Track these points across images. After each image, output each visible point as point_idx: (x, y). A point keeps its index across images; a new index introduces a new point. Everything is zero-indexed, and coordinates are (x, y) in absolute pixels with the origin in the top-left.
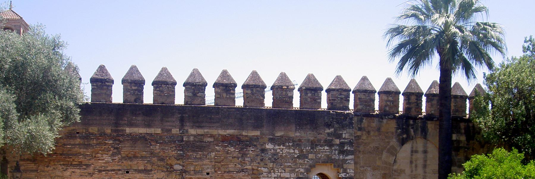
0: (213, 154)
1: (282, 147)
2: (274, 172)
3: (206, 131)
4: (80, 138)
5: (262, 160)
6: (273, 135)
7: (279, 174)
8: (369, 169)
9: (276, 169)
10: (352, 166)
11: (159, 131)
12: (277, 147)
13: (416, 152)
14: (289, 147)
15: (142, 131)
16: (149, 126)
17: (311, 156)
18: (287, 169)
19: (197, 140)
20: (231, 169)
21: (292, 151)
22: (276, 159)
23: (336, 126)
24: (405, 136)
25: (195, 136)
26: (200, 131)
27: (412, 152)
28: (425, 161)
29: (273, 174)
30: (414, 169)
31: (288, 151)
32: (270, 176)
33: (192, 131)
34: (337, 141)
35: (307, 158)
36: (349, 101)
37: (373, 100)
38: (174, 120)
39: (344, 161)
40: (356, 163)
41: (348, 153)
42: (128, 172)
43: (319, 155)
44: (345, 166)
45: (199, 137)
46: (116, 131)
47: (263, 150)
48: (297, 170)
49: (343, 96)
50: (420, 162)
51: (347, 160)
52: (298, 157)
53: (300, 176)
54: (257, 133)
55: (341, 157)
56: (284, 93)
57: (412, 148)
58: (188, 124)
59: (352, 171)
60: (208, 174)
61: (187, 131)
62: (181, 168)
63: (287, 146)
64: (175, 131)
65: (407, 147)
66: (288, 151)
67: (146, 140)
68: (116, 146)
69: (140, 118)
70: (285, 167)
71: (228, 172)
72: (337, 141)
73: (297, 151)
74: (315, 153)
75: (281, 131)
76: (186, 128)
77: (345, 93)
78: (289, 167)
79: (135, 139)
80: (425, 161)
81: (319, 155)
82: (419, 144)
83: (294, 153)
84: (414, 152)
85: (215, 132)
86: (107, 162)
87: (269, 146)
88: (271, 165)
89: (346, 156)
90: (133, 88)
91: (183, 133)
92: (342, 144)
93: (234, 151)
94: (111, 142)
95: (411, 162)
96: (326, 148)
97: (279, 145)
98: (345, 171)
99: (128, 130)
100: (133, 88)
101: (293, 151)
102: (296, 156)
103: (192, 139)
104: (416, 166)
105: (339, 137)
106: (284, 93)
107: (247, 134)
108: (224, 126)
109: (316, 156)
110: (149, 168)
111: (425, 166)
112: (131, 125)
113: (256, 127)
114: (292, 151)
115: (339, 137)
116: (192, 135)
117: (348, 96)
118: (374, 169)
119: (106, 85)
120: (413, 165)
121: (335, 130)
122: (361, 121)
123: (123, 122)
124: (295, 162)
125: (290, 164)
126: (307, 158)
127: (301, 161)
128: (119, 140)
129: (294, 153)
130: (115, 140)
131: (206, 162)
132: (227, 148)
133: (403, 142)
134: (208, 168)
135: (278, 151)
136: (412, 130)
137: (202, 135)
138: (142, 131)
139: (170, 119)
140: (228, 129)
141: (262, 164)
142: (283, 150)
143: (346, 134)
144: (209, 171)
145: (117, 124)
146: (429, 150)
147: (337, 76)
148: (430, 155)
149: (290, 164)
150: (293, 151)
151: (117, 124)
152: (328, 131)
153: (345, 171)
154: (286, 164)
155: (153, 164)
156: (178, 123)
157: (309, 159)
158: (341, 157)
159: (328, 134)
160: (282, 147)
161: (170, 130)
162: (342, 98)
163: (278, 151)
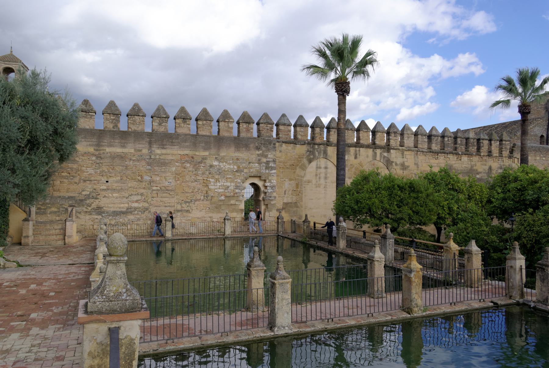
0: (174, 169)
1: (224, 164)
5: (210, 173)
6: (219, 155)
7: (222, 183)
8: (287, 180)
9: (220, 180)
10: (275, 178)
11: (132, 151)
12: (221, 164)
13: (320, 168)
14: (230, 164)
16: (123, 147)
17: (245, 171)
18: (229, 180)
22: (221, 172)
23: (264, 149)
24: (312, 157)
25: (160, 155)
26: (164, 151)
27: (317, 168)
28: (326, 174)
30: (318, 180)
31: (229, 166)
33: (158, 151)
34: (264, 160)
35: (243, 171)
36: (272, 131)
37: (290, 131)
38: (144, 142)
39: (269, 174)
40: (277, 176)
41: (272, 168)
43: (252, 170)
44: (270, 178)
47: (211, 166)
48: (236, 180)
49: (268, 128)
50: (323, 175)
51: (271, 173)
52: (236, 171)
54: (207, 153)
55: (267, 171)
57: (317, 165)
58: (155, 146)
59: (274, 181)
61: (154, 151)
62: (150, 178)
64: (145, 151)
65: (314, 164)
66: (229, 166)
71: (185, 182)
72: (264, 160)
73: (236, 167)
76: (153, 149)
77: (270, 126)
78: (230, 178)
79: (114, 157)
80: (326, 174)
81: (252, 170)
82: (322, 162)
84: (318, 167)
85: (175, 152)
86: (91, 174)
87: (216, 163)
88: (217, 177)
89: (271, 170)
90: (112, 117)
91: (151, 152)
92: (268, 163)
95: (316, 175)
96: (257, 165)
97: (222, 163)
98: (270, 181)
99: (108, 150)
100: (112, 117)
103: (158, 157)
104: (320, 178)
105: (266, 156)
111: (326, 178)
112: (110, 146)
113: (205, 149)
114: (232, 167)
115: (266, 156)
117: (272, 128)
118: (291, 180)
119: (89, 115)
120: (318, 177)
121: (263, 152)
122: (281, 146)
123: (104, 144)
126: (243, 171)
131: (169, 174)
132: (185, 164)
133: (310, 161)
135: (222, 166)
136: (317, 153)
139: (141, 142)
141: (210, 176)
142: (225, 166)
143: (271, 156)
146: (329, 167)
147: (264, 114)
148: (329, 170)
151: (98, 145)
152: (258, 152)
153: (270, 181)
156: (147, 145)
158: (267, 171)
159: (258, 155)
160: (224, 164)
161: (140, 151)
162: (268, 129)
163: (222, 166)
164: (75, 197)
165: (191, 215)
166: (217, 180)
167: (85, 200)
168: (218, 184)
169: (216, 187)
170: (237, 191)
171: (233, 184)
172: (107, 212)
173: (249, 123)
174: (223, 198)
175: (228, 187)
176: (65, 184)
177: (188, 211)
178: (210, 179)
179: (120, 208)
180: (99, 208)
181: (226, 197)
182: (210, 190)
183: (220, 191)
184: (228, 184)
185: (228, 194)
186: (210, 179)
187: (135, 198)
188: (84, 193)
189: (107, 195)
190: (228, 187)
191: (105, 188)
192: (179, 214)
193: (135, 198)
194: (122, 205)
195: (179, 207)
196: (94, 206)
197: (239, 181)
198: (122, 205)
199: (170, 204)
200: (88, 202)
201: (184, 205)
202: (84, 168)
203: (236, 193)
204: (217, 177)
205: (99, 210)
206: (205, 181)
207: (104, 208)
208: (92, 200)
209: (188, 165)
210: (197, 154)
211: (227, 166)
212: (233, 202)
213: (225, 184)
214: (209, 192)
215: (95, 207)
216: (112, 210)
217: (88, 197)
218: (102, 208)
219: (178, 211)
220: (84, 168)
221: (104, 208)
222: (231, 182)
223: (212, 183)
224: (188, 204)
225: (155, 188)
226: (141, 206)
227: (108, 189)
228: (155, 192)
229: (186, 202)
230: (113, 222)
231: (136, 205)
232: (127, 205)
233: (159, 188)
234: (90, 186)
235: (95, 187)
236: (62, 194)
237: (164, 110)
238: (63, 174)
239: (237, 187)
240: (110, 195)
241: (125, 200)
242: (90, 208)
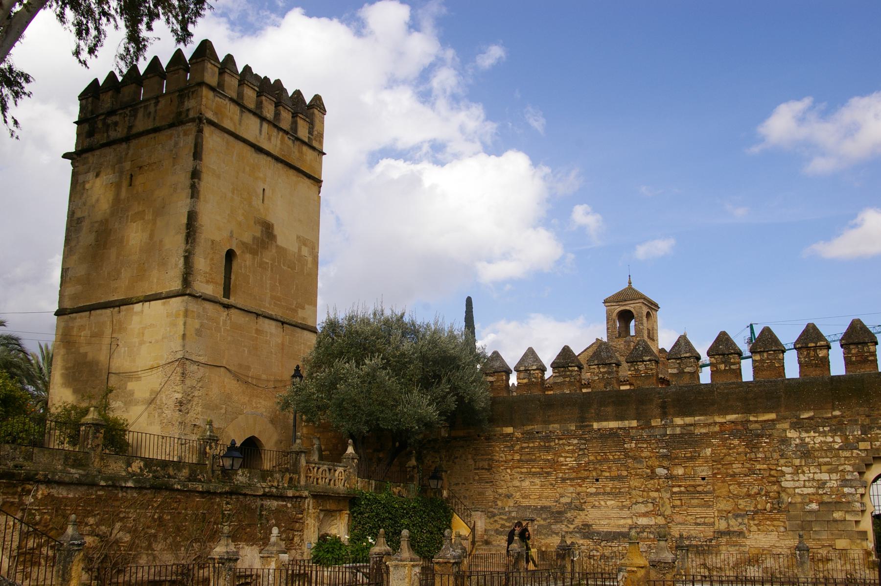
0: (708, 451)
1: (812, 434)
2: (803, 473)
3: (697, 418)
4: (540, 438)
7: (811, 475)
9: (805, 469)
12: (804, 435)
14: (824, 434)
15: (613, 424)
16: (622, 418)
17: (862, 445)
18: (824, 468)
19: (685, 432)
20: (737, 471)
21: (830, 439)
22: (806, 453)
26: (688, 420)
29: (801, 475)
31: (823, 439)
32: (796, 478)
33: (678, 421)
42: (597, 480)
45: (689, 428)
46: (581, 427)
48: (841, 468)
53: (847, 477)
56: (812, 353)
60: (703, 479)
63: (820, 432)
66: (823, 439)
67: (618, 436)
68: (582, 447)
69: (609, 409)
70: (819, 465)
73: (838, 439)
74: (871, 440)
75: (810, 409)
78: (825, 464)
83: (834, 442)
87: (791, 434)
88: (797, 462)
93: (739, 445)
94: (576, 441)
97: (807, 432)
99: (596, 426)
101: (831, 440)
102: (837, 447)
103: (678, 431)
106: (812, 353)
107: (755, 419)
108: (724, 412)
109: (871, 445)
110: (625, 473)
112: (599, 419)
114: (830, 439)
116: (678, 426)
119: (569, 371)
124: (838, 456)
125: (828, 459)
127: (847, 454)
128: (585, 439)
129: (834, 442)
130: (581, 439)
134: (703, 471)
135: (807, 440)
137: (691, 425)
138: (613, 424)
140: (728, 414)
141: (782, 461)
142: (814, 439)
144: (704, 474)
145: (582, 419)
149: (828, 459)
150: (831, 440)
151: (582, 419)
154: (821, 460)
155: (627, 468)
157: (861, 450)
160: (812, 434)
163: (807, 440)
164: (550, 507)
165: (748, 543)
166: (797, 470)
167: (565, 512)
168: (802, 477)
169: (797, 484)
170: (846, 490)
171: (834, 476)
172: (599, 533)
173: (865, 343)
174: (814, 506)
175: (825, 483)
176: (537, 487)
177: (740, 534)
178: (784, 468)
179: (619, 526)
180: (587, 525)
181: (821, 503)
182: (784, 489)
183: (806, 491)
184: (825, 477)
185: (826, 499)
186: (784, 468)
187: (642, 509)
188: (563, 500)
189: (597, 504)
190: (825, 483)
191: (593, 490)
192: (723, 540)
193: (642, 509)
194: (622, 522)
195: (722, 525)
196: (578, 522)
197: (849, 468)
198: (622, 522)
199: (707, 520)
200: (569, 515)
201: (732, 522)
202: (562, 459)
203: (844, 495)
204: (797, 462)
205: (586, 531)
206: (773, 472)
207: (594, 527)
208: (575, 513)
209: (736, 442)
210: (752, 418)
211: (819, 439)
212: (837, 515)
213: (817, 477)
214: (783, 495)
215: (580, 524)
216: (606, 529)
217: (569, 506)
218: (591, 525)
219: (722, 533)
220: (562, 459)
221: (594, 527)
222: (830, 472)
223: (788, 477)
224: (740, 520)
225: (676, 489)
226: (652, 523)
227: (599, 494)
228: (677, 497)
229: (736, 516)
230: (607, 552)
231: (643, 521)
232: (629, 521)
233: (683, 489)
234: (571, 489)
235: (579, 489)
236: (532, 503)
237: (688, 343)
238: (533, 470)
239: (845, 482)
240: (602, 503)
241: (625, 513)
242: (572, 526)
